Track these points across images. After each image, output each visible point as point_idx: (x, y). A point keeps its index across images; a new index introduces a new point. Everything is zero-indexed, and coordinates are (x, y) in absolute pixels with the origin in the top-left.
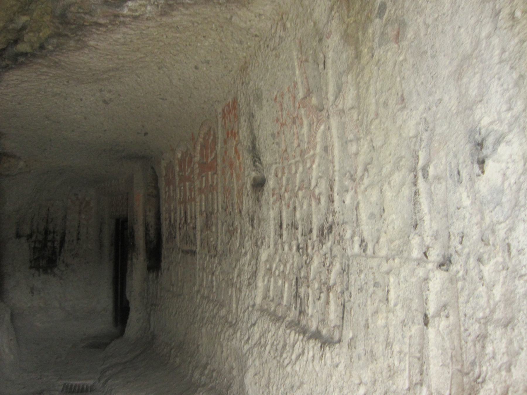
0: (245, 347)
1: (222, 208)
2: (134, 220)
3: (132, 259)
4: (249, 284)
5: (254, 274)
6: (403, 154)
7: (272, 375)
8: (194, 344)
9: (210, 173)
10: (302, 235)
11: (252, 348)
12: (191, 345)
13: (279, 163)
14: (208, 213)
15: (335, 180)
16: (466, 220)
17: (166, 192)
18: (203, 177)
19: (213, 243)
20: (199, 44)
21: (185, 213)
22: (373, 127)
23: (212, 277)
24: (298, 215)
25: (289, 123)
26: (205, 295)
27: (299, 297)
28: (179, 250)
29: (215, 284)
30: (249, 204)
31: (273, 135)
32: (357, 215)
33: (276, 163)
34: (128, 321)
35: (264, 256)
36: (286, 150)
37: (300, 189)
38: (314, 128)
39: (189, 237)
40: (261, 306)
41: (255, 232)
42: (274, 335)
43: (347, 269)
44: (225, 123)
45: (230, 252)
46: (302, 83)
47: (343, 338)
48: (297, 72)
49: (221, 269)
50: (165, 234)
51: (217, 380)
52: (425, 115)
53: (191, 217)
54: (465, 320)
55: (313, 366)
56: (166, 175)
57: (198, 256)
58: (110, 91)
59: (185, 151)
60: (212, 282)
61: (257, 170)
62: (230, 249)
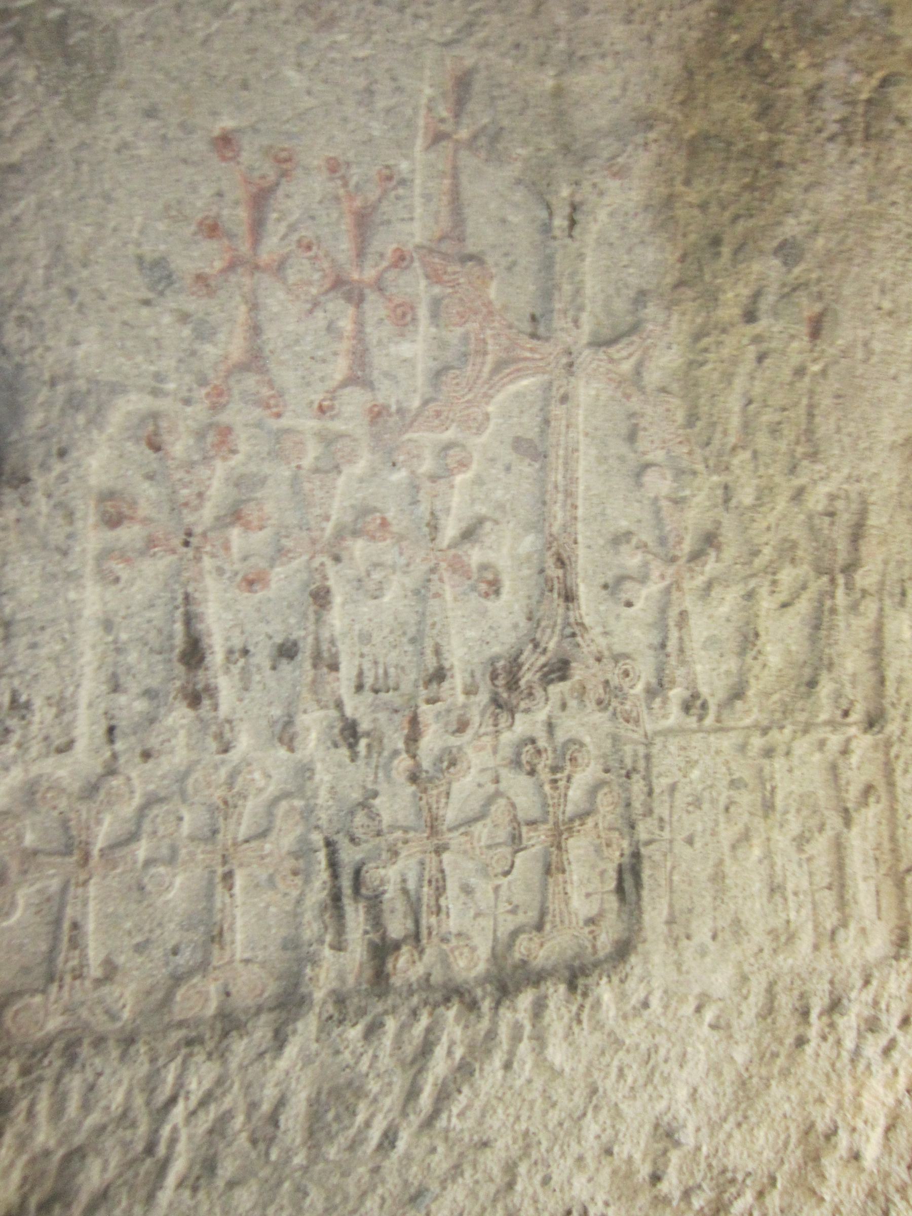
6: (794, 536)
10: (359, 688)
15: (576, 542)
22: (735, 461)
24: (337, 618)
32: (681, 639)
43: (642, 764)
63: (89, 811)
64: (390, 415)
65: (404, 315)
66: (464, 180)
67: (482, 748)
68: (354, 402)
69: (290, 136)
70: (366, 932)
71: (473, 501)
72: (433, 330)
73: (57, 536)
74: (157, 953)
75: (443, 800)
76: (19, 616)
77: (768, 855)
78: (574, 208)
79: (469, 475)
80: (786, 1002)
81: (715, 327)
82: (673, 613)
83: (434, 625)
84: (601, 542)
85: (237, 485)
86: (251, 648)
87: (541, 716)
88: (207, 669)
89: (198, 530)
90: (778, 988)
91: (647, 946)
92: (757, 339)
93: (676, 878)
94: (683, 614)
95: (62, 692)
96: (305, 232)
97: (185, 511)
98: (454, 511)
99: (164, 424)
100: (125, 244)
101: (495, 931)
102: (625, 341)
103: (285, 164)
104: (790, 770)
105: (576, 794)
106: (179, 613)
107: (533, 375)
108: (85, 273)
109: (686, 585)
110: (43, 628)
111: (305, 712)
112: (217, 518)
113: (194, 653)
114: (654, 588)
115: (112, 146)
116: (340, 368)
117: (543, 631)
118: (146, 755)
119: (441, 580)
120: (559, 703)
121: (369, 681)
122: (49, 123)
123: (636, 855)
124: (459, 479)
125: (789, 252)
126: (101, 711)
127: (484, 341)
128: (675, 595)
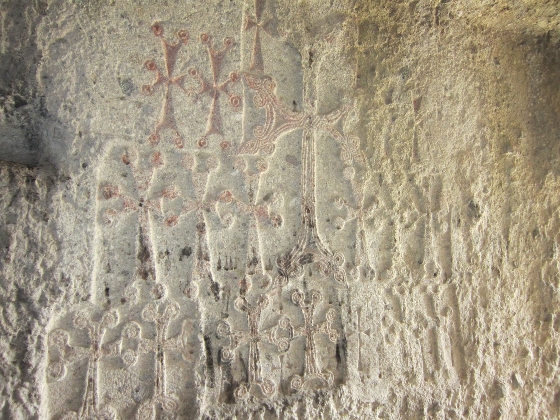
10: (219, 268)
32: (362, 243)
63: (97, 327)
64: (230, 146)
65: (236, 102)
66: (262, 43)
67: (274, 294)
68: (215, 141)
69: (186, 25)
70: (223, 379)
71: (268, 183)
72: (250, 108)
73: (82, 203)
74: (129, 392)
75: (257, 318)
76: (65, 239)
78: (311, 54)
79: (267, 171)
80: (412, 404)
81: (373, 106)
82: (358, 231)
83: (252, 239)
84: (326, 200)
85: (163, 178)
86: (170, 251)
87: (301, 278)
88: (150, 261)
89: (146, 199)
90: (409, 399)
91: (350, 382)
92: (392, 110)
93: (362, 350)
94: (362, 232)
95: (84, 274)
96: (192, 67)
97: (140, 190)
98: (259, 188)
99: (130, 152)
100: (112, 73)
101: (281, 377)
102: (334, 112)
103: (184, 37)
104: (412, 300)
106: (137, 237)
107: (294, 127)
108: (94, 86)
110: (75, 245)
111: (195, 279)
112: (155, 193)
113: (145, 254)
116: (208, 126)
117: (300, 242)
118: (123, 301)
119: (254, 219)
120: (308, 273)
121: (223, 265)
122: (78, 21)
123: (345, 341)
124: (261, 174)
125: (405, 73)
126: (102, 282)
127: (272, 113)
128: (358, 223)
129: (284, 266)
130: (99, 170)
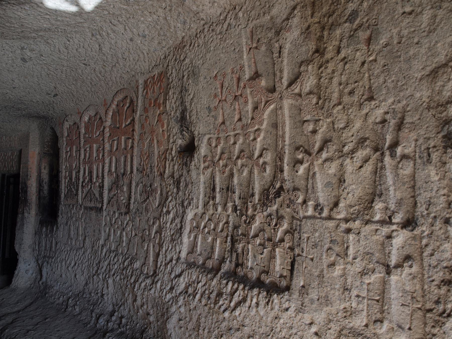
0: (168, 296)
1: (137, 170)
2: (27, 176)
3: (23, 213)
4: (173, 240)
5: (180, 231)
7: (203, 320)
8: (97, 293)
9: (123, 137)
10: (240, 198)
11: (177, 296)
12: (93, 295)
13: (214, 134)
14: (119, 174)
15: (285, 153)
16: (434, 192)
17: (67, 152)
18: (114, 140)
19: (124, 201)
20: (142, 19)
21: (91, 173)
22: (335, 111)
23: (121, 233)
24: (236, 180)
25: (230, 100)
26: (113, 248)
27: (236, 251)
28: (81, 206)
29: (124, 239)
30: (174, 169)
31: (209, 109)
32: (313, 183)
33: (209, 134)
34: (16, 272)
35: (190, 215)
36: (223, 123)
37: (238, 158)
38: (262, 107)
39: (95, 195)
40: (187, 260)
41: (180, 193)
42: (204, 285)
44: (147, 93)
45: (147, 210)
46: (249, 66)
47: (293, 286)
48: (245, 57)
49: (133, 225)
50: (63, 191)
51: (127, 325)
52: (393, 107)
53: (98, 176)
54: (429, 269)
55: (257, 311)
56: (68, 136)
57: (105, 213)
58: (32, 50)
59: (93, 115)
60: (121, 236)
61: (183, 139)
62: (146, 208)
77: (344, 275)
82: (311, 173)
87: (275, 207)
105: (279, 234)
109: (315, 163)
114: (305, 165)
115: (201, 88)
121: (242, 196)
129: (266, 198)
130: (203, 151)
